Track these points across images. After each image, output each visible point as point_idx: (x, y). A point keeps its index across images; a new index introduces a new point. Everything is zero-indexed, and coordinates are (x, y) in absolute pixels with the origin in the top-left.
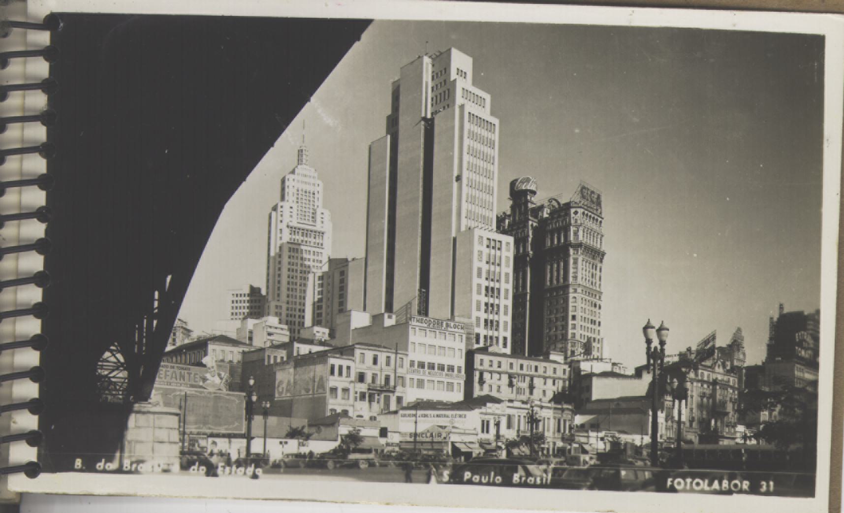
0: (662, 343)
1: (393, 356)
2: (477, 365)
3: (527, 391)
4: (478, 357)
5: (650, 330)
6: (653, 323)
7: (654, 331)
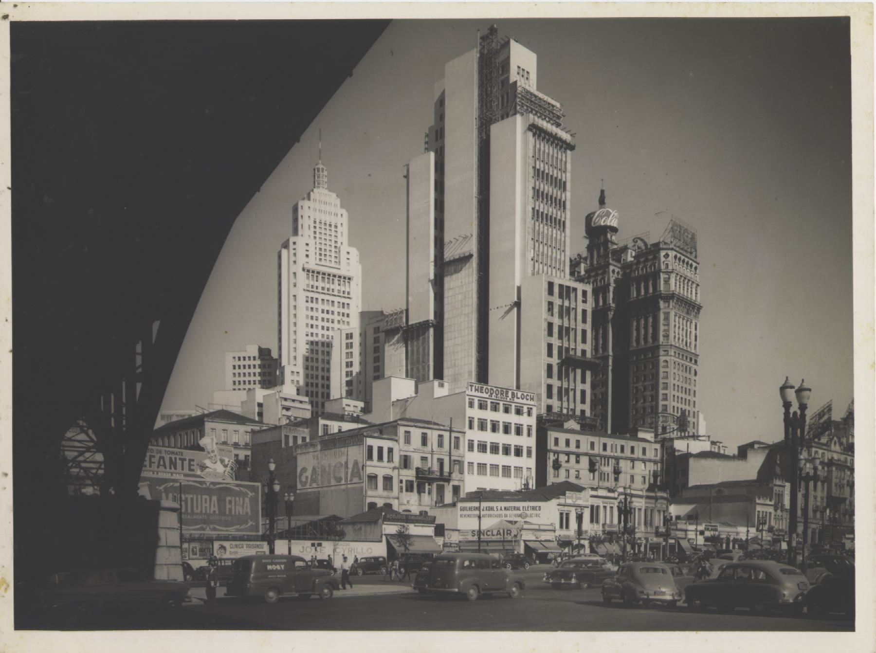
0: (803, 407)
1: (446, 435)
2: (551, 445)
3: (612, 477)
4: (552, 435)
5: (789, 390)
6: (791, 382)
7: (793, 390)
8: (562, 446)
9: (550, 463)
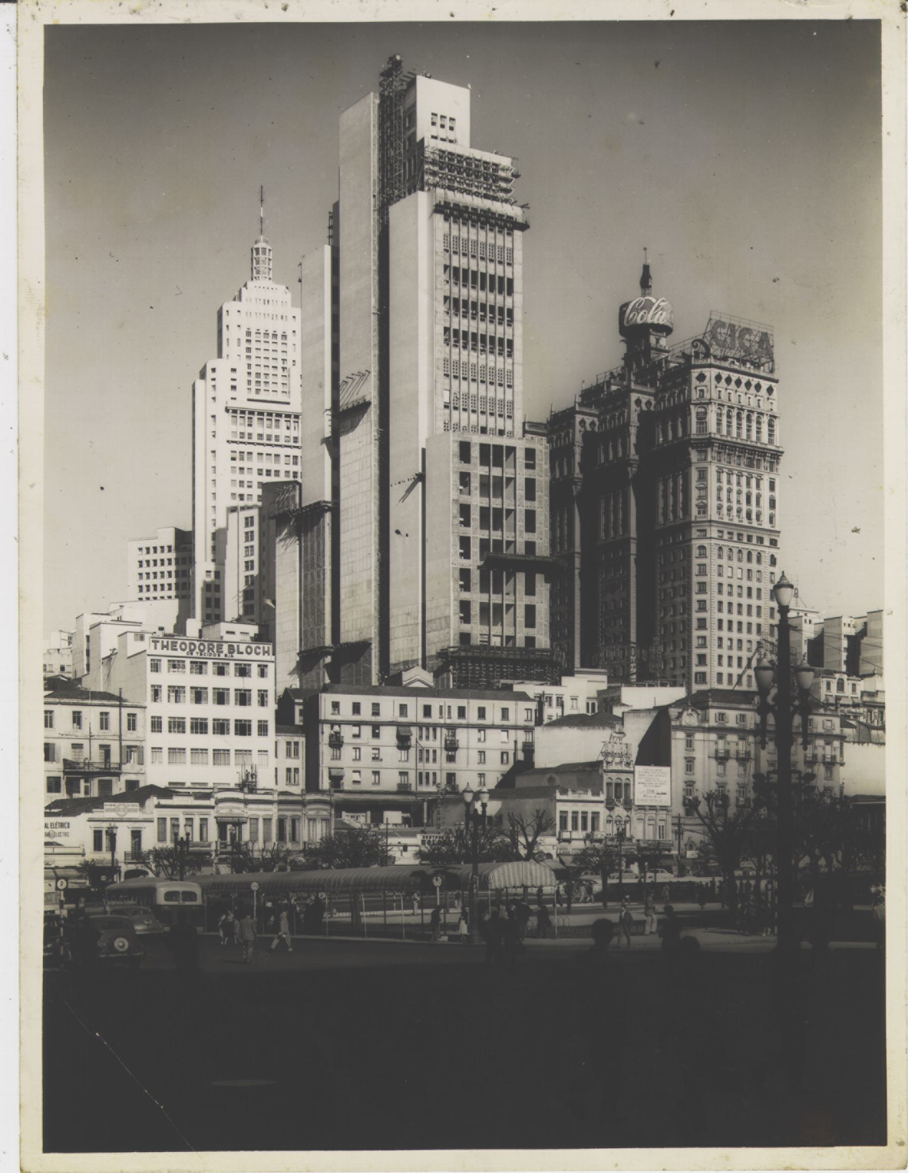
2: (326, 711)
3: (442, 755)
8: (346, 712)
9: (324, 739)
